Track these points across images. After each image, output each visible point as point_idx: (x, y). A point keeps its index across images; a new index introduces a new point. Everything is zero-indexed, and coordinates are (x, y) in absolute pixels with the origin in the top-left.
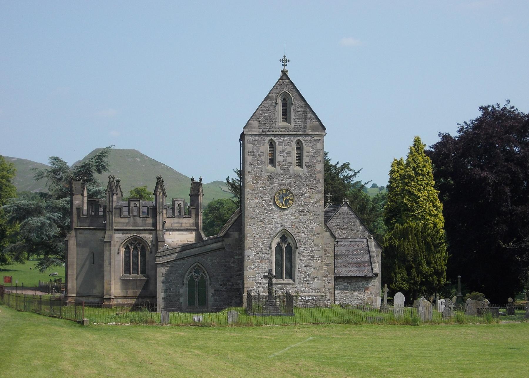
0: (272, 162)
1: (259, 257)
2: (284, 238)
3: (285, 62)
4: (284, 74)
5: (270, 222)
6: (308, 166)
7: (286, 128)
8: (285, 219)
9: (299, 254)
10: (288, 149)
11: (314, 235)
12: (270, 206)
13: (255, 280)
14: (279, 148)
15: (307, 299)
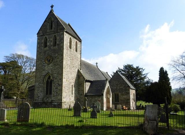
1: (40, 85)
3: (52, 7)
4: (51, 12)
5: (44, 70)
7: (51, 32)
9: (54, 83)
10: (51, 39)
11: (60, 74)
12: (44, 63)
13: (38, 95)
14: (48, 40)
15: (55, 104)
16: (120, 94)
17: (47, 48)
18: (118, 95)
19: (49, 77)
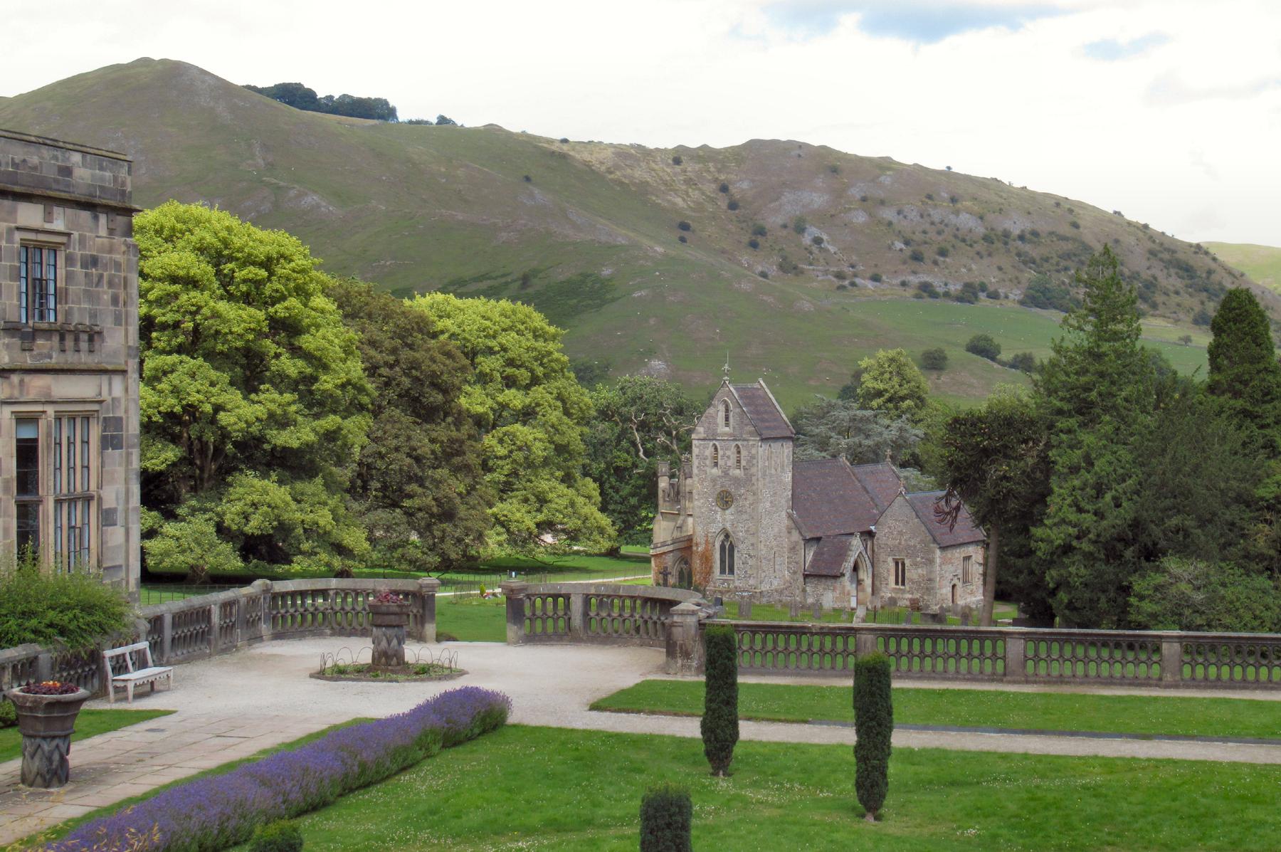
0: (716, 464)
2: (727, 536)
6: (745, 469)
8: (725, 518)
10: (728, 453)
14: (720, 453)
16: (907, 562)
17: (715, 471)
18: (903, 564)
19: (727, 536)
